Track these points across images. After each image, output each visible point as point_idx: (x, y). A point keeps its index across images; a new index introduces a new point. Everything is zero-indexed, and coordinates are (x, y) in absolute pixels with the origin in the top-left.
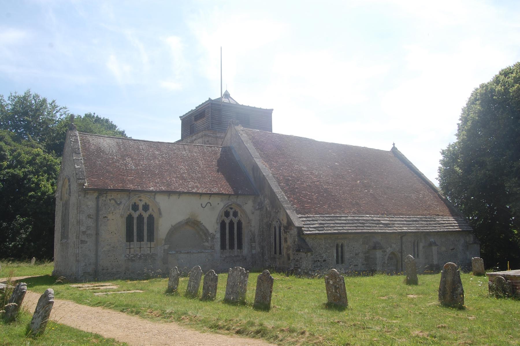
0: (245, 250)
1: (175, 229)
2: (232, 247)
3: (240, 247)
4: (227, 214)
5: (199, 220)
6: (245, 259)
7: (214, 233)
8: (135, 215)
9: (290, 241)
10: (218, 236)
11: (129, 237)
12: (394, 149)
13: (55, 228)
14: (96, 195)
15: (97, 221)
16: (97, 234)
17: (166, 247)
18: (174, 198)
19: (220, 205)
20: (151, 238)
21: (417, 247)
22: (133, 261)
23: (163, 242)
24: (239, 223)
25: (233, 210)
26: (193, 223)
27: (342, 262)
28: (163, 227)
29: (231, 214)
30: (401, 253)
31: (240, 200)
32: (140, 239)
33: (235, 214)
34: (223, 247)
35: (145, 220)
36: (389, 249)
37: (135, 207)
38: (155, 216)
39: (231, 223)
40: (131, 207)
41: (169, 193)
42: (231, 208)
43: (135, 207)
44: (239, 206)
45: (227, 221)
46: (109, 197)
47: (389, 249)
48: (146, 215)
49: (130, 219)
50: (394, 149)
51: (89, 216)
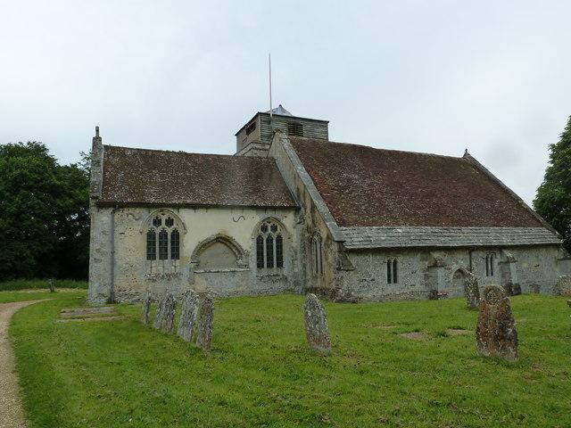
0: (285, 271)
1: (204, 246)
2: (270, 265)
3: (280, 265)
4: (264, 229)
5: (230, 236)
6: (286, 278)
7: (250, 250)
8: (158, 230)
9: (330, 257)
11: (151, 256)
12: (466, 154)
13: (93, 246)
14: (111, 210)
15: (113, 237)
16: (113, 253)
17: (193, 265)
18: (201, 212)
20: (176, 255)
21: (491, 260)
22: (154, 281)
23: (189, 260)
24: (279, 240)
25: (271, 224)
27: (395, 281)
28: (189, 245)
29: (269, 228)
32: (163, 256)
33: (274, 229)
34: (260, 265)
35: (169, 237)
37: (157, 222)
38: (181, 231)
39: (270, 240)
40: (152, 222)
41: (194, 207)
42: (269, 223)
43: (157, 222)
45: (265, 238)
46: (125, 212)
48: (169, 231)
49: (151, 235)
50: (466, 154)
51: (104, 232)
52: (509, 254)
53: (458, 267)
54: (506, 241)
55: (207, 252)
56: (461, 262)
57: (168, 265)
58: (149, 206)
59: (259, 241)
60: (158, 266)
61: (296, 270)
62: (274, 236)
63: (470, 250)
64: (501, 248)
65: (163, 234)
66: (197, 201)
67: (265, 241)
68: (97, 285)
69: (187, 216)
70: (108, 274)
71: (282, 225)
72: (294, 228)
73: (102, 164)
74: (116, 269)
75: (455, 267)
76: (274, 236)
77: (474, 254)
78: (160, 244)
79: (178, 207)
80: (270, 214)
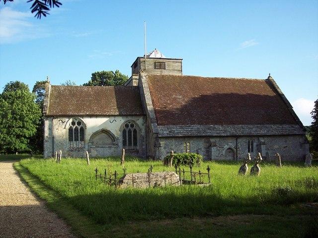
0: (138, 148)
1: (95, 134)
2: (130, 144)
3: (135, 144)
4: (127, 126)
10: (121, 139)
11: (71, 139)
19: (121, 121)
20: (83, 139)
22: (72, 151)
24: (135, 131)
26: (105, 131)
30: (236, 149)
31: (134, 119)
32: (76, 140)
33: (132, 126)
35: (79, 130)
36: (226, 146)
39: (130, 132)
41: (91, 116)
42: (129, 123)
44: (133, 121)
47: (226, 146)
52: (262, 140)
53: (228, 147)
54: (263, 132)
55: (97, 137)
56: (231, 144)
57: (80, 144)
58: (69, 116)
59: (124, 132)
60: (74, 144)
61: (144, 147)
62: (132, 130)
63: (237, 137)
64: (258, 136)
65: (76, 129)
66: (92, 113)
67: (127, 132)
68: (47, 152)
69: (86, 121)
70: (51, 148)
71: (137, 124)
72: (143, 125)
73: (49, 96)
74: (55, 145)
75: (226, 147)
76: (132, 130)
77: (239, 140)
78: (75, 133)
79: (83, 116)
80: (130, 118)
